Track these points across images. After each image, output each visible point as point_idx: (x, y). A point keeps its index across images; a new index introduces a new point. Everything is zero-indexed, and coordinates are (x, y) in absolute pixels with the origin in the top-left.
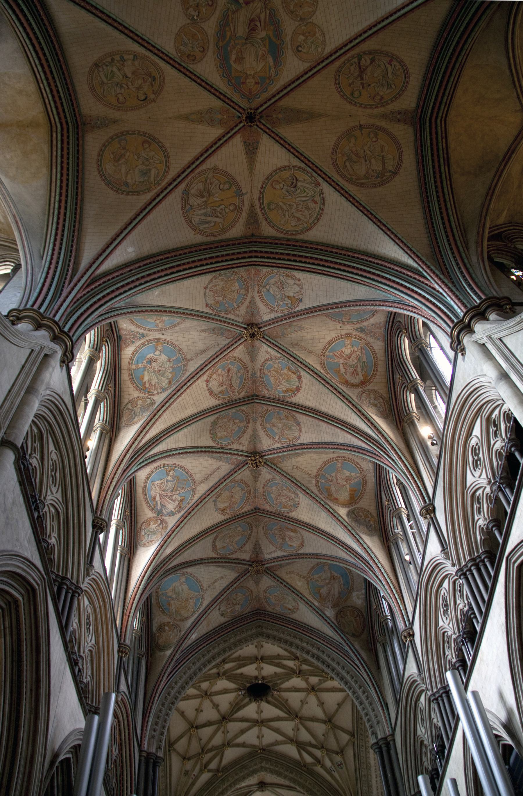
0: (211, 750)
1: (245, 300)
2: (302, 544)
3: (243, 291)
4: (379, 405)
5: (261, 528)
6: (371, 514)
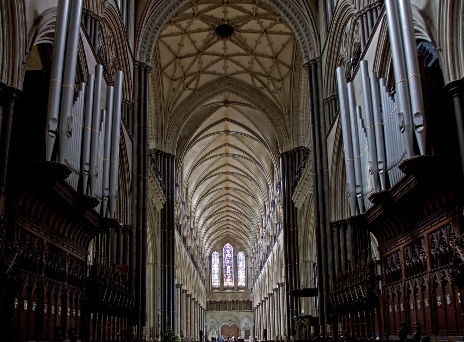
0: (191, 75)
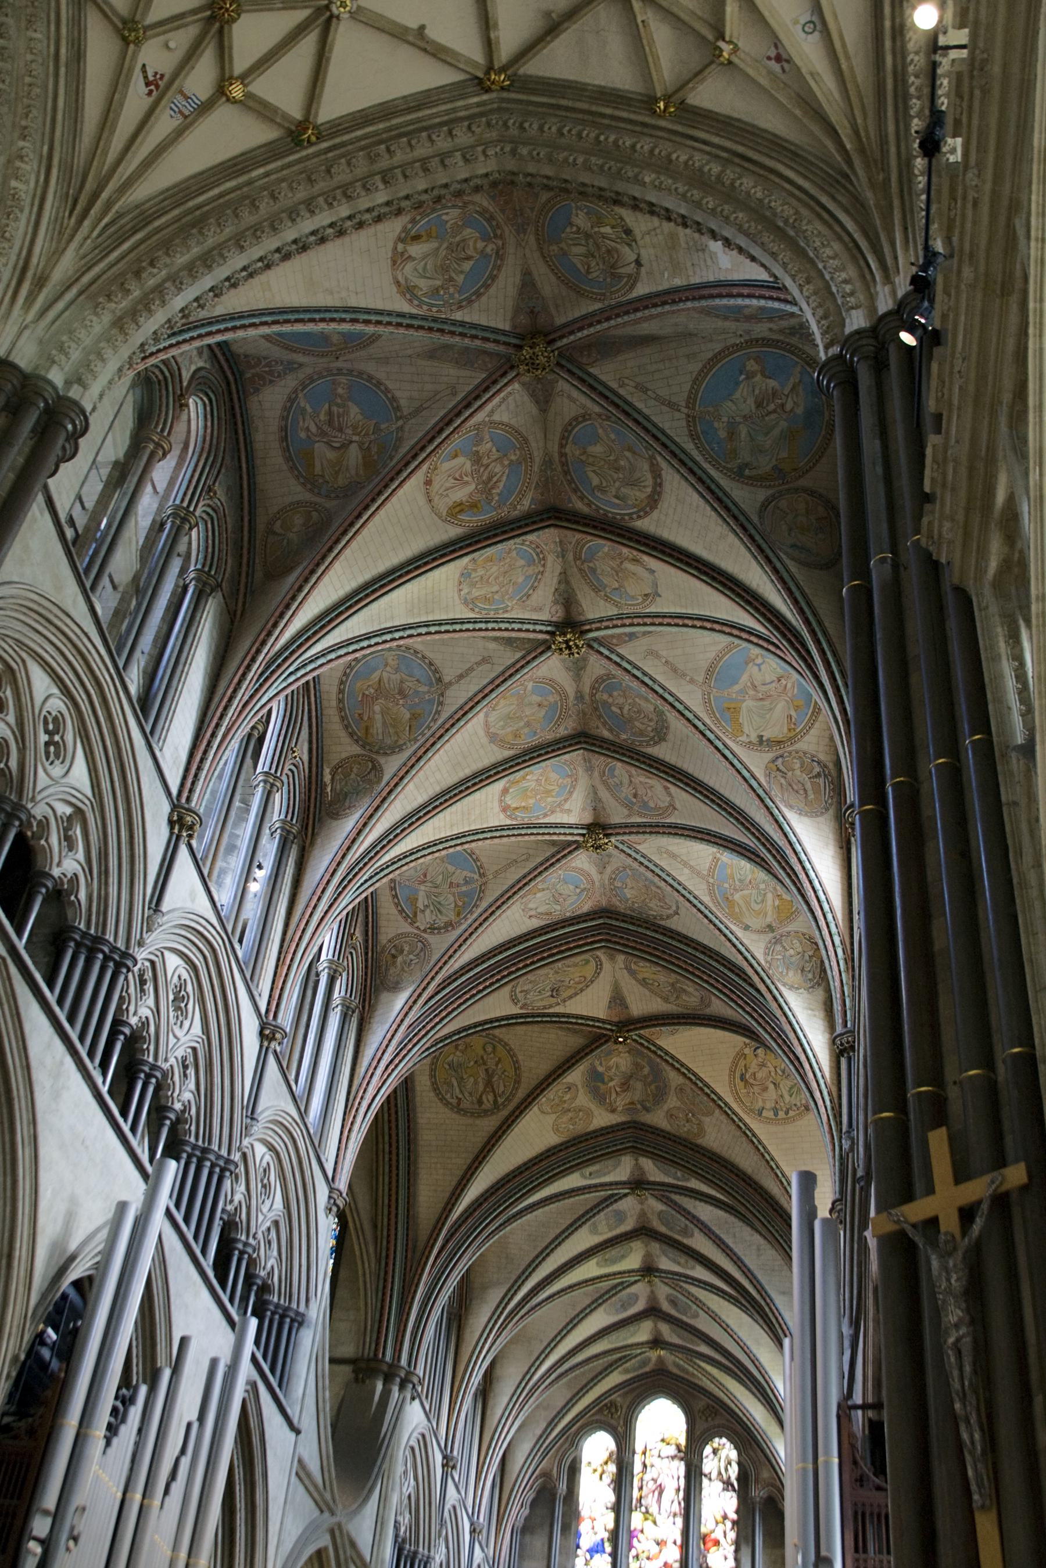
2: (428, 483)
5: (538, 456)
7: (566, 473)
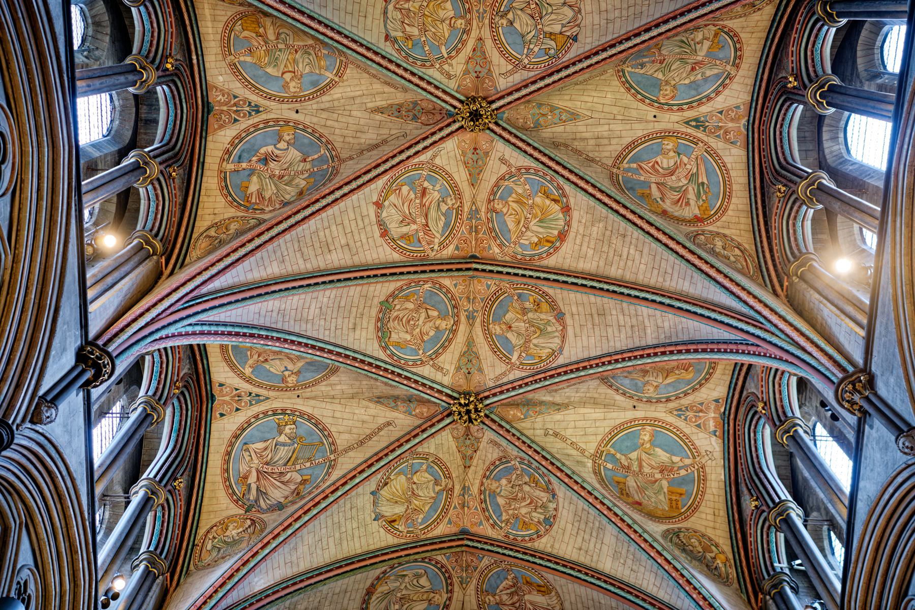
1: (464, 43)
3: (460, 23)
4: (732, 259)
6: (717, 546)
7: (450, 577)
